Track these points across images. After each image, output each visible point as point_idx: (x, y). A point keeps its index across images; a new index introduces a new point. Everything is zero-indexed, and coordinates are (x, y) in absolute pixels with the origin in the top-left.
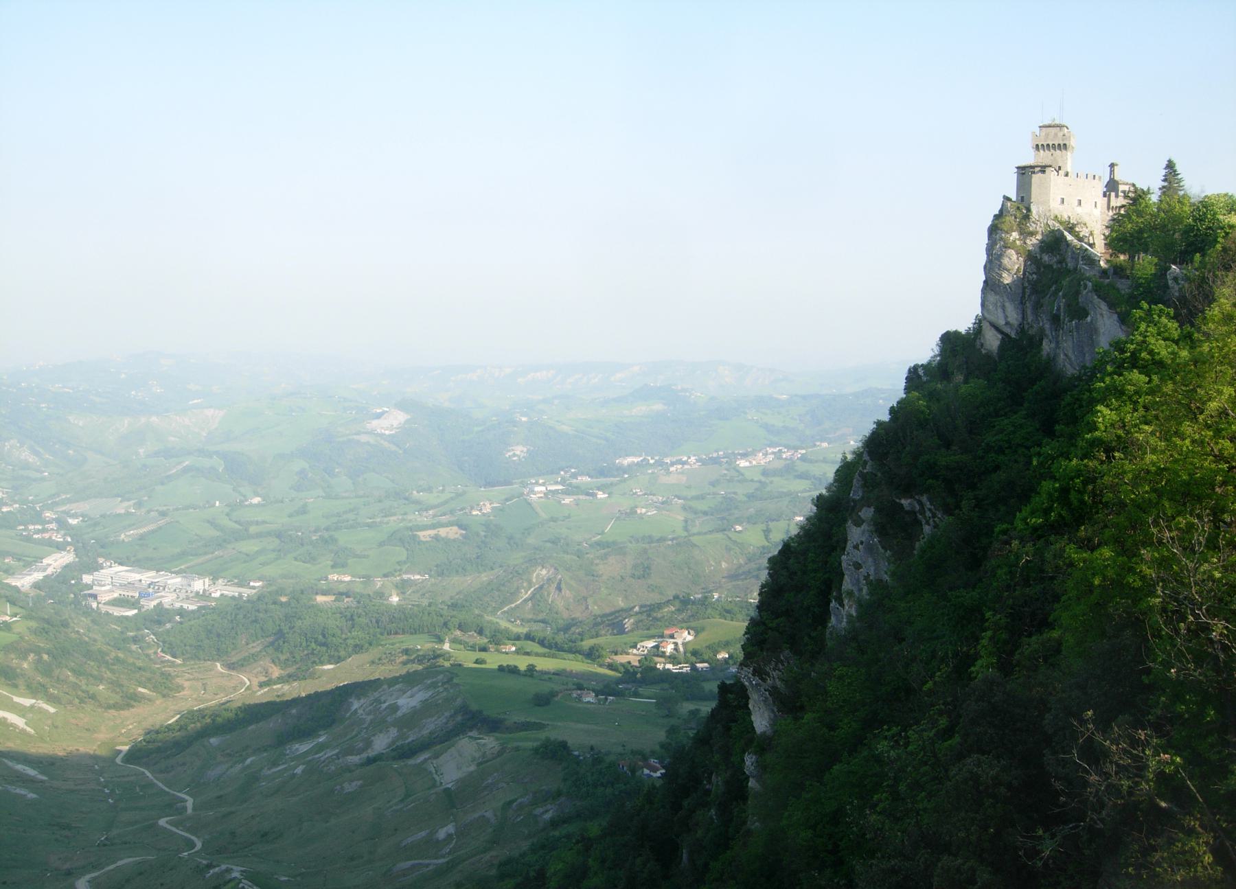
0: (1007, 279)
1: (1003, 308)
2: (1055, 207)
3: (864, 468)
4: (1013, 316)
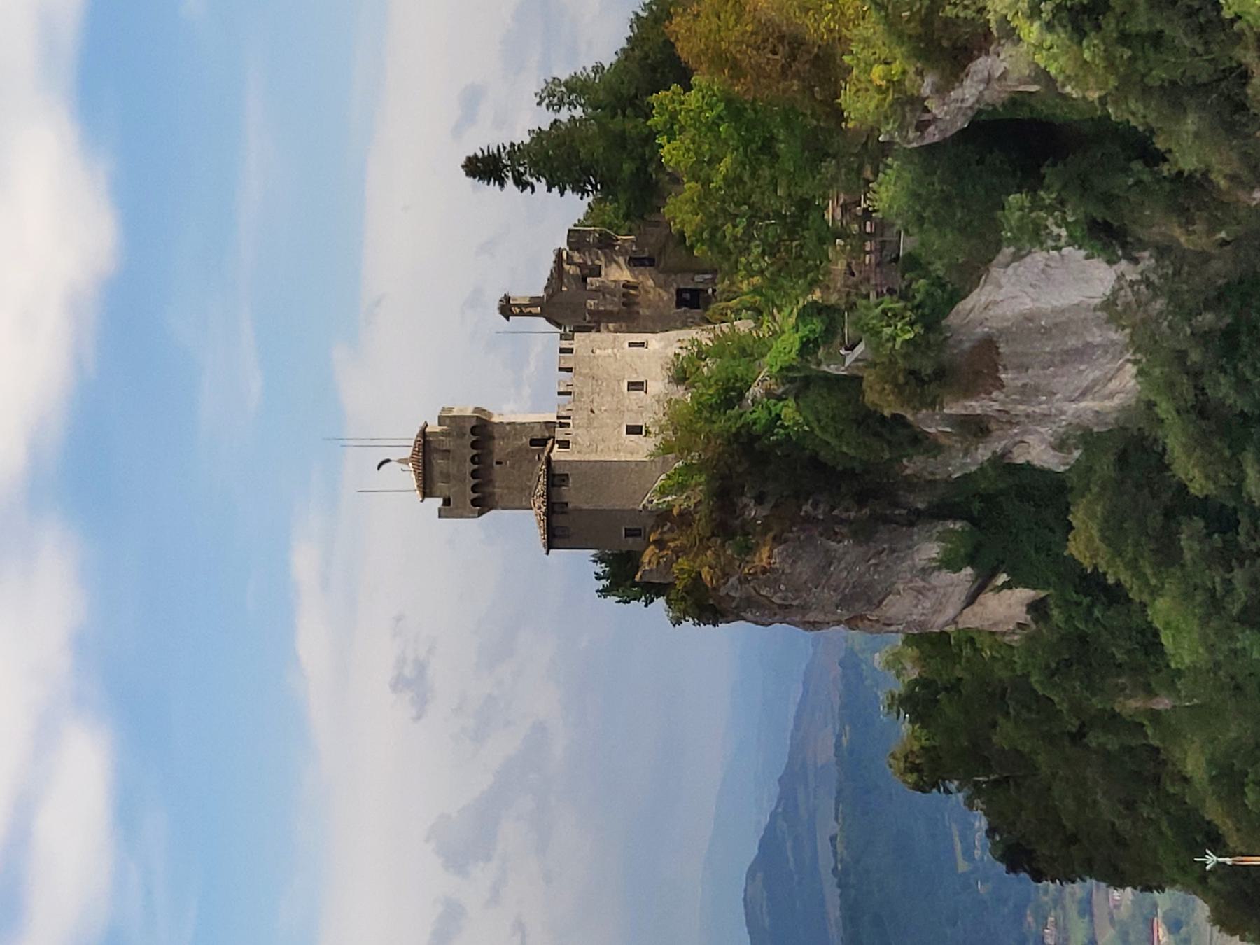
2: (641, 449)
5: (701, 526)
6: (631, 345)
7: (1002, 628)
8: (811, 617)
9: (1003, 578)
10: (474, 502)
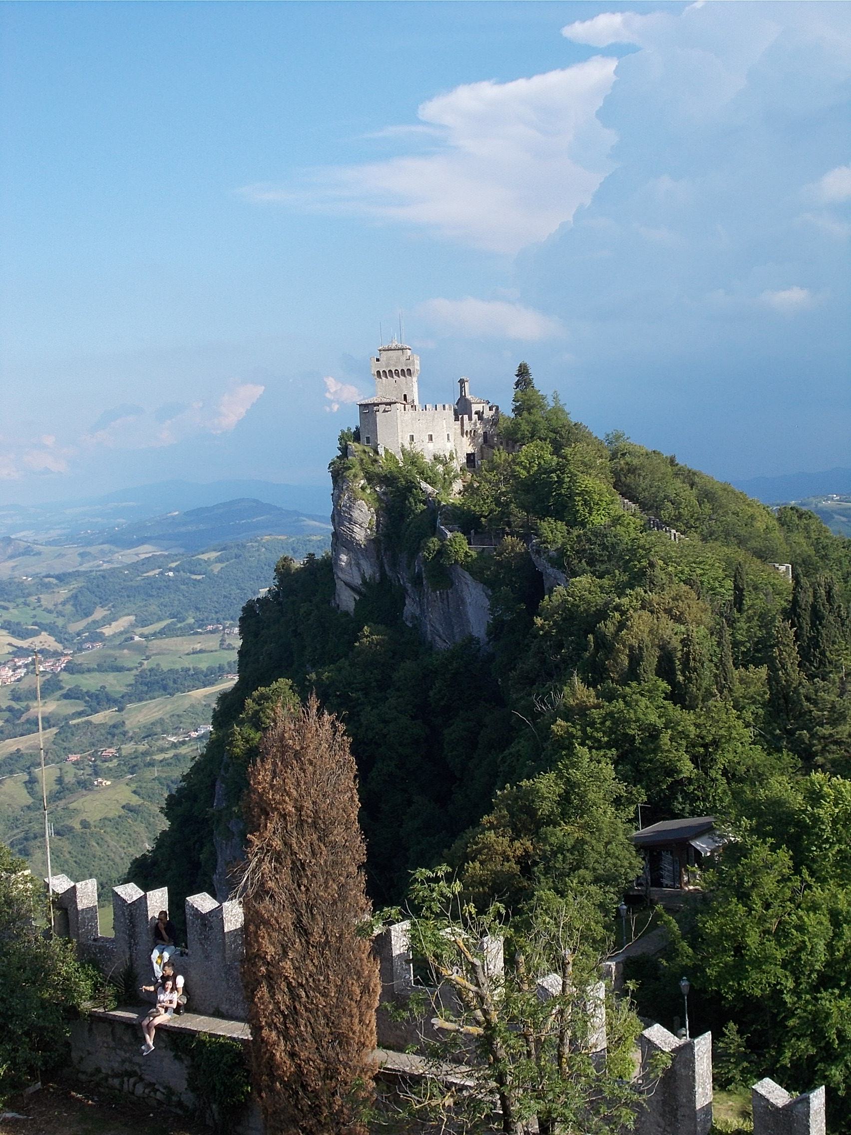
0: (360, 535)
1: (358, 565)
3: (227, 771)
4: (368, 569)
5: (371, 469)
7: (337, 598)
8: (336, 517)
9: (358, 598)
10: (378, 372)
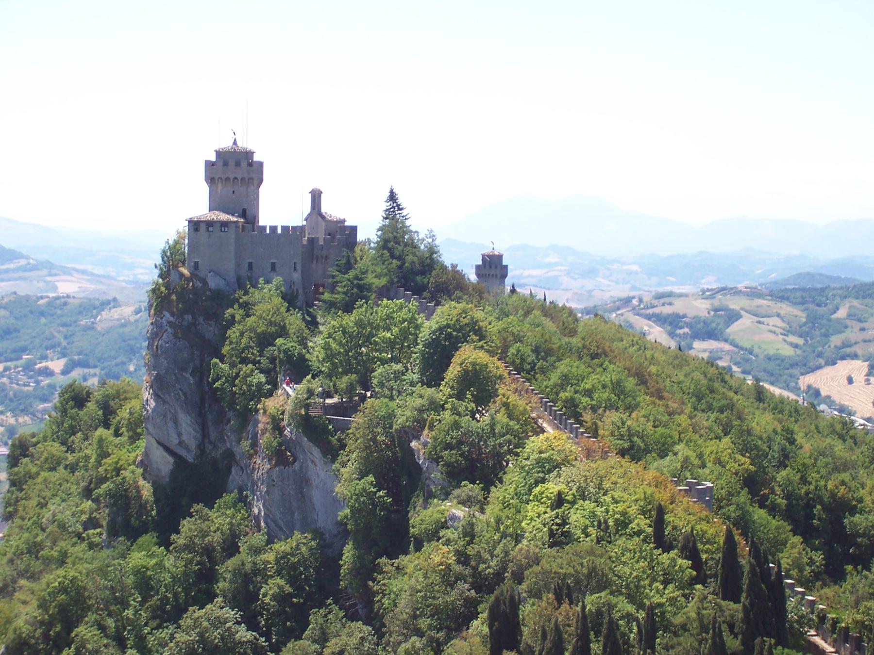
6: (295, 263)
